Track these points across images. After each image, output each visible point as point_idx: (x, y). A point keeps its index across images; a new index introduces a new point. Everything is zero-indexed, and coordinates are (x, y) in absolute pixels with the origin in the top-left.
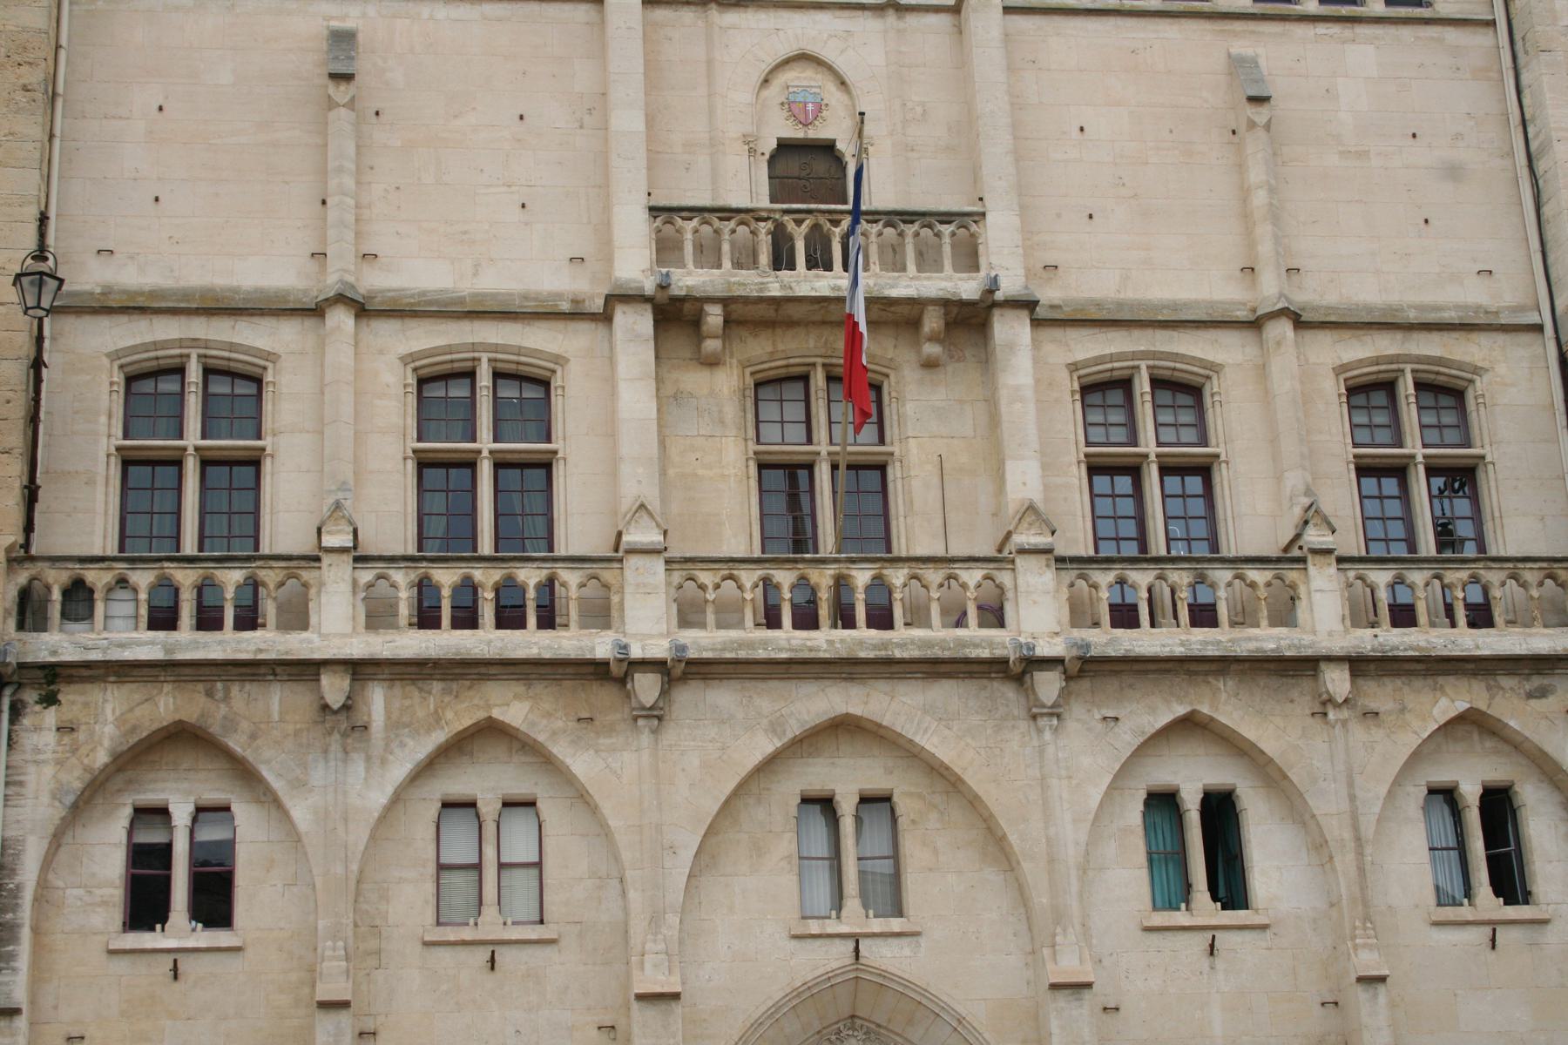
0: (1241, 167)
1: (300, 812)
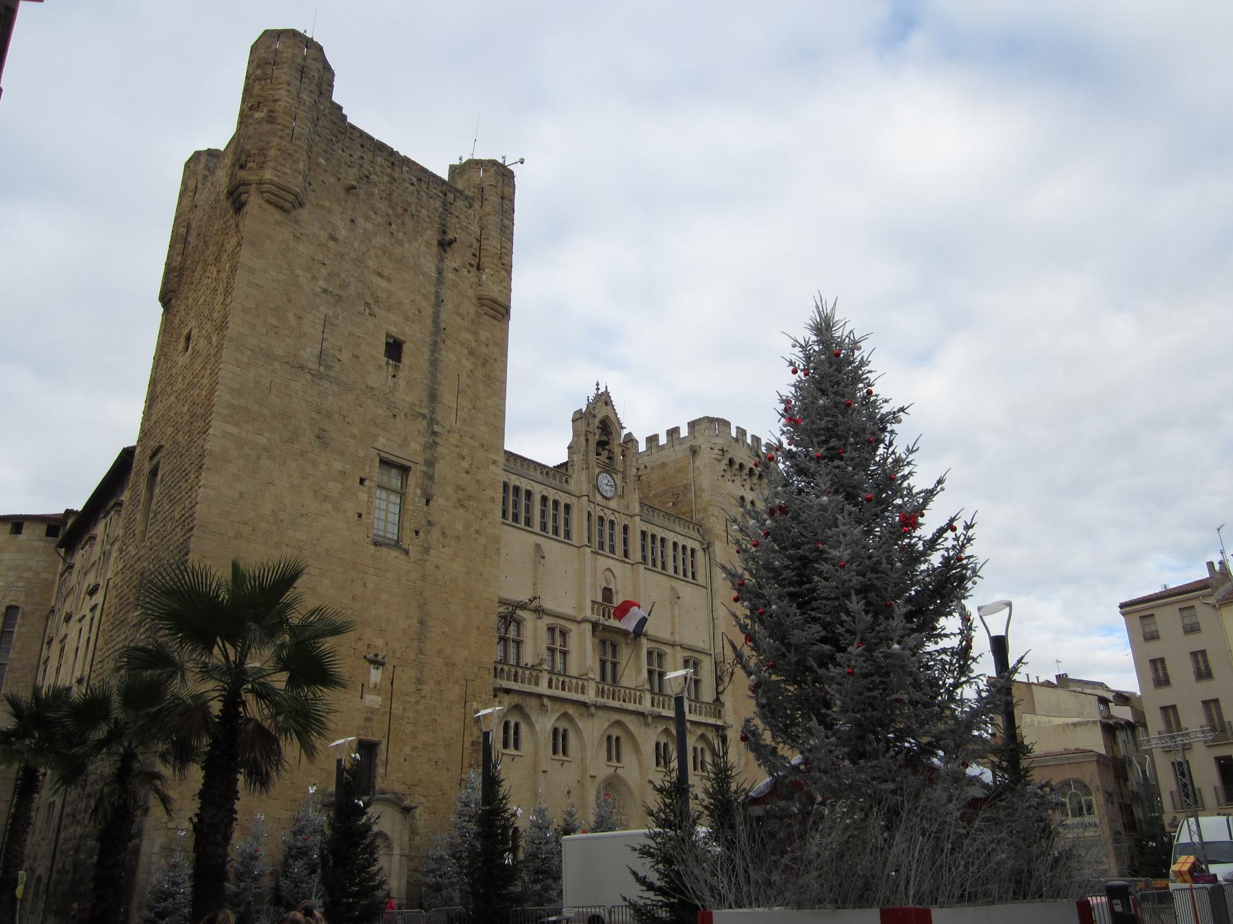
0: (672, 610)
1: (538, 727)
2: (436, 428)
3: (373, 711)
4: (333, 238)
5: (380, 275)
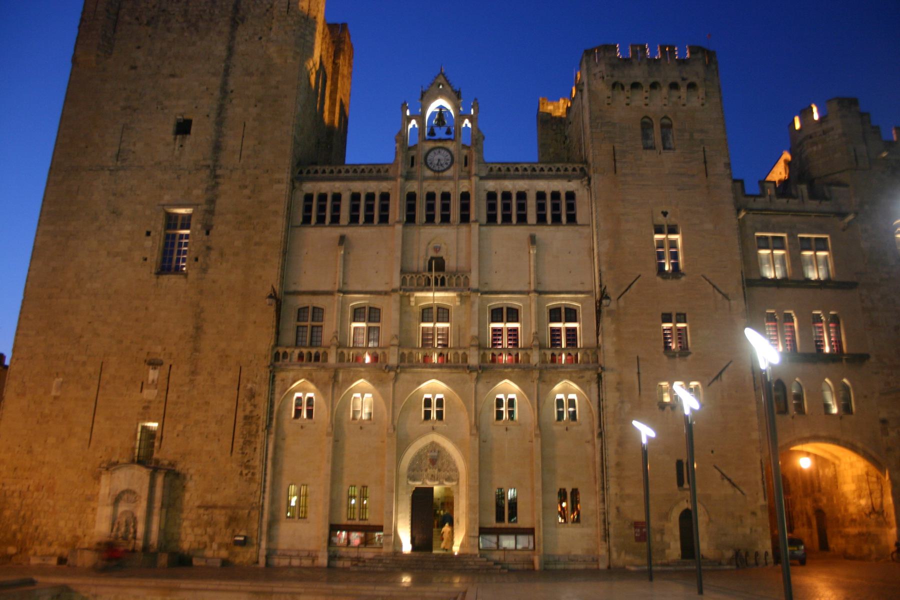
2: (219, 172)
3: (150, 402)
4: (134, 68)
5: (173, 76)
